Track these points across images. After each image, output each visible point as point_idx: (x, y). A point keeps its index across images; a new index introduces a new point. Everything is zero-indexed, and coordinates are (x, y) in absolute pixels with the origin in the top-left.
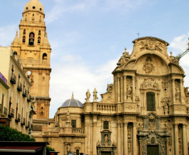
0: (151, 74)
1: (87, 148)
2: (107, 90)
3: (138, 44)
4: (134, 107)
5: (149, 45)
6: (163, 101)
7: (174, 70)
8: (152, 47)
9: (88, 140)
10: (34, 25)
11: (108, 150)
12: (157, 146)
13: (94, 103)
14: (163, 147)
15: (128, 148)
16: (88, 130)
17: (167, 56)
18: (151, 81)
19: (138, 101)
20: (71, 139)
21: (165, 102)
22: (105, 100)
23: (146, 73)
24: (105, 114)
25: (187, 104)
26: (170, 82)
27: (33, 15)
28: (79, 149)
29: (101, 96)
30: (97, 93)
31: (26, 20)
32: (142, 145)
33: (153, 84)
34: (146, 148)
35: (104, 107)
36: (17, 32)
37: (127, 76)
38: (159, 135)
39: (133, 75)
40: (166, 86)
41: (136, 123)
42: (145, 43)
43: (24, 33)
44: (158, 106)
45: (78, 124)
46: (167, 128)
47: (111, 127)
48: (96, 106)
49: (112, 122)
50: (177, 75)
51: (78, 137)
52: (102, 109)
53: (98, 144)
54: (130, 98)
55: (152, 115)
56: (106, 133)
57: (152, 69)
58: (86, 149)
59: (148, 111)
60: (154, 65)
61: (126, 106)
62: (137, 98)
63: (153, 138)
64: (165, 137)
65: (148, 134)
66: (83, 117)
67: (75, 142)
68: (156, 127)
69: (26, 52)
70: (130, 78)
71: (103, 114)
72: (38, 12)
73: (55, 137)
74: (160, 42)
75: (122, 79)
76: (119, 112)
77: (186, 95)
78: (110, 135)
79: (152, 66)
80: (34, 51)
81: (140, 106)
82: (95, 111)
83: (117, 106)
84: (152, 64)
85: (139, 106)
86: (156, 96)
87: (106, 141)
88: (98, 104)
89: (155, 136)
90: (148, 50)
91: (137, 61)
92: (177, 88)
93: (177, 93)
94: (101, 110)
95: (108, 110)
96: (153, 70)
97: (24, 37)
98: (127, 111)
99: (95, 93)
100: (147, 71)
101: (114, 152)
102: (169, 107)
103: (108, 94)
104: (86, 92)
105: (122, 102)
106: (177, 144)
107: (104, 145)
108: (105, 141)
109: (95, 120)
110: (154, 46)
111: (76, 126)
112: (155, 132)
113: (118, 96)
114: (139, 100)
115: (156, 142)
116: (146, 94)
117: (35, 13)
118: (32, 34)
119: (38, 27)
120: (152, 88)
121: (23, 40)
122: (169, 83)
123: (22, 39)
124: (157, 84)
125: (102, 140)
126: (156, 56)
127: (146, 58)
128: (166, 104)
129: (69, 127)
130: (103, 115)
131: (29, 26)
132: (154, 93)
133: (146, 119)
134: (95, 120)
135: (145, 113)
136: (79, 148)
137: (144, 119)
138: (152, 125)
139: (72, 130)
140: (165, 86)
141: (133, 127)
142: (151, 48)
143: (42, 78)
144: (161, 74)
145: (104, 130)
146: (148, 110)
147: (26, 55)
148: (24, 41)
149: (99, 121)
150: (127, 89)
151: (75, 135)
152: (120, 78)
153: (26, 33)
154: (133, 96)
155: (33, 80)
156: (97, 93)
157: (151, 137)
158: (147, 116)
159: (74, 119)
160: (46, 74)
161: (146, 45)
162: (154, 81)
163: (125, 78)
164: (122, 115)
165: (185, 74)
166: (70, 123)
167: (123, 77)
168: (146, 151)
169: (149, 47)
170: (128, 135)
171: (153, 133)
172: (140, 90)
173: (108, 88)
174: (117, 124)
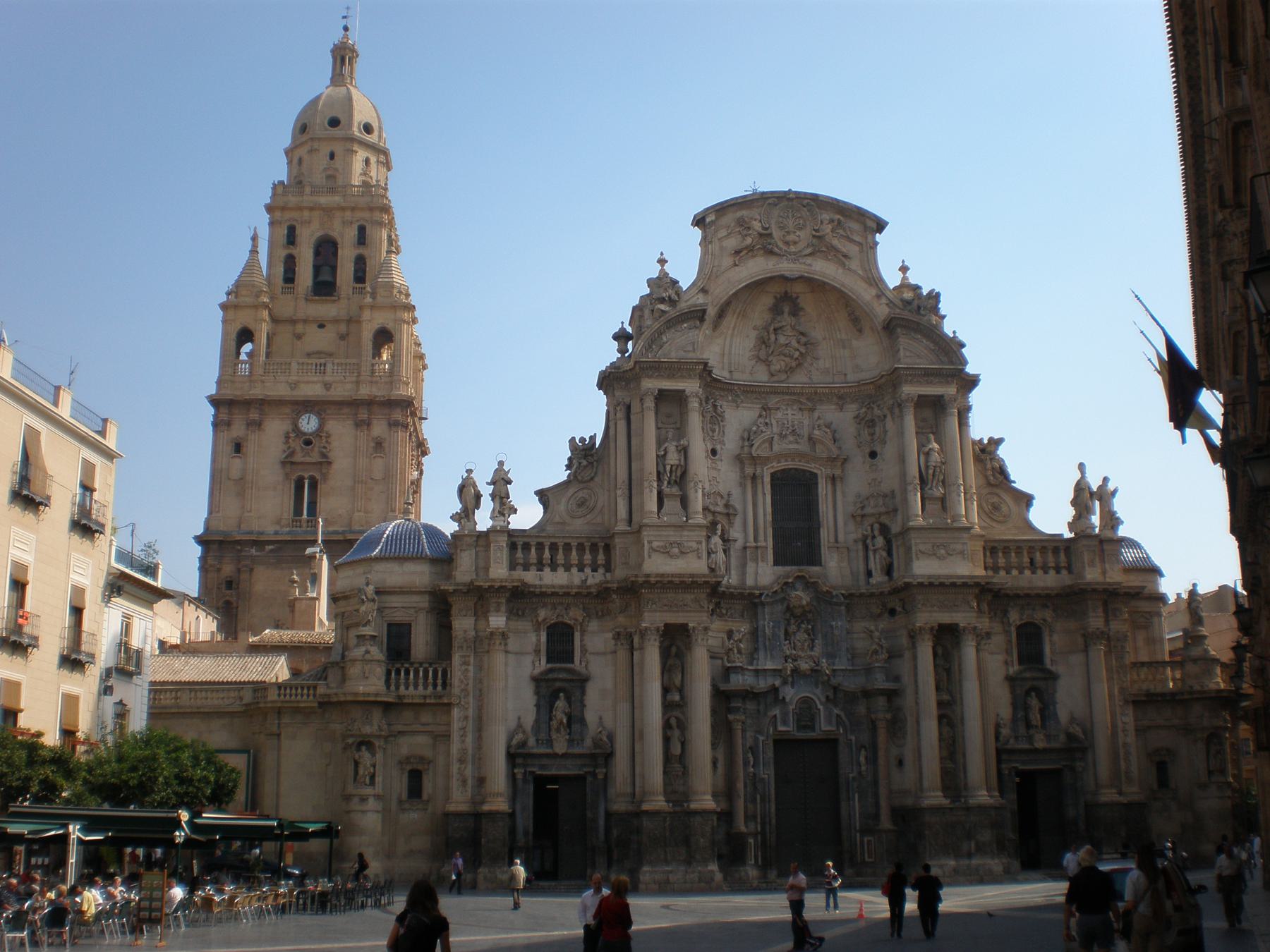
0: (799, 379)
1: (462, 761)
2: (568, 467)
3: (723, 233)
4: (694, 545)
5: (777, 234)
6: (859, 512)
7: (912, 353)
8: (795, 243)
9: (466, 718)
10: (337, 199)
11: (570, 769)
12: (830, 743)
13: (492, 537)
14: (864, 747)
15: (667, 758)
16: (460, 667)
17: (875, 280)
18: (799, 416)
19: (728, 515)
20: (377, 715)
21: (873, 515)
22: (557, 519)
23: (772, 375)
24: (553, 586)
25: (994, 524)
26: (892, 413)
27: (332, 156)
28: (420, 767)
29: (540, 500)
30: (510, 482)
31: (300, 182)
32: (744, 738)
33: (805, 432)
34: (770, 754)
35: (547, 554)
36: (254, 239)
37: (660, 391)
38: (835, 689)
39: (691, 386)
40: (876, 437)
41: (706, 629)
42: (757, 226)
43: (291, 238)
44: (836, 541)
45: (421, 642)
46: (876, 652)
47: (584, 651)
48: (500, 548)
49: (593, 625)
50: (928, 375)
51: (418, 707)
52: (540, 566)
53: (519, 737)
54: (679, 504)
55: (798, 585)
56: (558, 684)
57: (801, 354)
58: (455, 768)
59: (780, 567)
60: (817, 333)
61: (650, 542)
62: (721, 503)
63: (806, 703)
64: (867, 694)
65: (777, 683)
66: (441, 605)
67: (401, 733)
69: (300, 328)
70: (679, 398)
71: (541, 587)
72: (352, 140)
73: (297, 710)
74: (838, 217)
75: (635, 408)
76: (620, 573)
77: (986, 477)
78: (583, 693)
79: (803, 340)
80: (336, 321)
81: (739, 544)
82: (499, 571)
83: (614, 547)
84: (802, 329)
86: (823, 489)
87: (561, 723)
88: (520, 542)
89: (818, 691)
91: (721, 315)
92: (929, 442)
93: (927, 467)
94: (534, 568)
95: (567, 568)
96: (809, 359)
97: (290, 263)
98: (656, 565)
99: (497, 483)
100: (778, 367)
101: (600, 777)
102: (889, 542)
103: (571, 491)
104: (460, 482)
105: (635, 526)
106: (930, 728)
107: (550, 742)
108: (554, 723)
109: (497, 621)
110: (804, 235)
111: (409, 650)
112: (816, 671)
113: (619, 492)
114: (731, 511)
115: (824, 726)
116: (767, 479)
117: (338, 149)
118: (326, 249)
119: (353, 209)
120: (804, 447)
121: (286, 272)
122: (889, 417)
123: (280, 270)
124: (828, 426)
125: (537, 721)
126: (817, 286)
127: (767, 301)
128: (876, 526)
129: (368, 657)
130: (543, 594)
131: (311, 209)
132: (811, 473)
134: (497, 621)
135: (764, 573)
136: (422, 759)
137: (760, 610)
138: (801, 636)
139: (388, 673)
140: (872, 434)
141: (689, 647)
142: (793, 249)
143: (373, 444)
144: (851, 377)
145: (549, 666)
146: (776, 563)
147: (299, 343)
148: (290, 277)
149: (524, 625)
150: (661, 459)
151: (399, 697)
152: (628, 408)
153: (298, 240)
154: (691, 494)
155: (329, 455)
156: (510, 482)
157: (790, 694)
158: (775, 592)
159: (399, 617)
160: (390, 425)
161: (765, 235)
162: (816, 414)
163: (650, 403)
164: (634, 591)
165: (970, 369)
166: (373, 637)
167: (641, 400)
168: (771, 772)
169: (781, 244)
170: (666, 690)
172: (739, 459)
173: (570, 459)
174: (617, 636)
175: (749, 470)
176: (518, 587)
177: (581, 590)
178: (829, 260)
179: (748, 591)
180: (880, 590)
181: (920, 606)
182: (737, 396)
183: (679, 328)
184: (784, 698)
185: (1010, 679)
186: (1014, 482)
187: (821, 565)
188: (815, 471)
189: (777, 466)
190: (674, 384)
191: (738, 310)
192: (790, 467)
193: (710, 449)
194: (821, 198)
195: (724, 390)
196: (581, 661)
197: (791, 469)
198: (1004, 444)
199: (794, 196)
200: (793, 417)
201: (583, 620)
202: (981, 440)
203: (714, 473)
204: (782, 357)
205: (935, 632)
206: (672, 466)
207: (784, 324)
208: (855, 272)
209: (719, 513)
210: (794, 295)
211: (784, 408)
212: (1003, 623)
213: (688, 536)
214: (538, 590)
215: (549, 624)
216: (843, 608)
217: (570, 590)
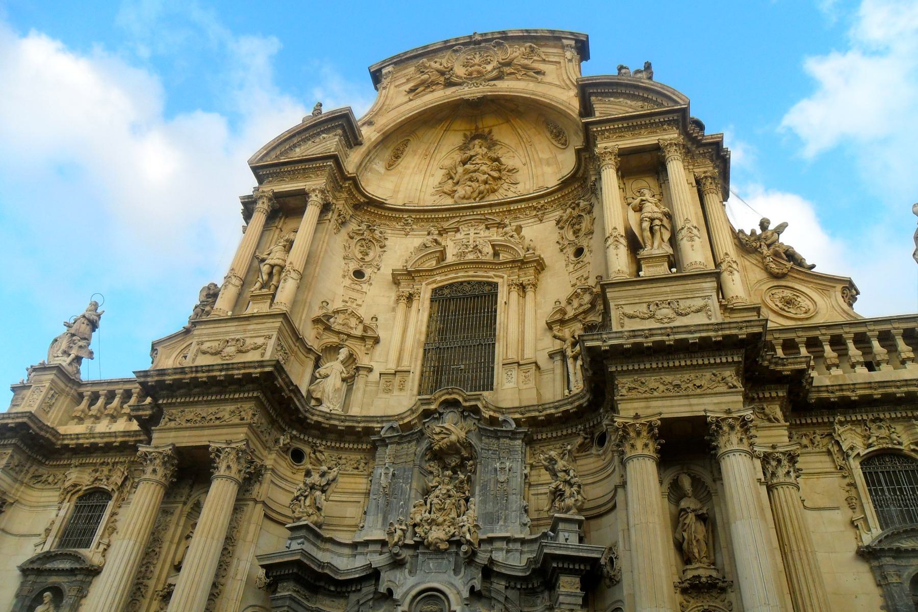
5: (460, 71)
50: (631, 124)
56: (53, 579)
65: (378, 560)
68: (484, 502)
85: (370, 370)
90: (453, 89)
114: (370, 333)
132: (489, 284)
133: (390, 449)
158: (408, 426)
171: (438, 552)
175: (406, 289)
176: (24, 424)
177: (127, 439)
178: (519, 80)
179: (362, 425)
180: (577, 404)
181: (624, 392)
182: (407, 224)
183: (317, 140)
184: (390, 592)
185: (866, 554)
186: (813, 266)
187: (492, 389)
188: (495, 280)
189: (441, 279)
190: (296, 185)
191: (420, 151)
192: (460, 280)
193: (353, 266)
194: (510, 35)
195: (390, 218)
196: (99, 543)
197: (462, 283)
198: (786, 229)
199: (480, 38)
200: (476, 235)
201: (123, 483)
202: (753, 233)
203: (355, 295)
204: (469, 183)
205: (656, 431)
206: (272, 266)
207: (472, 153)
208: (550, 84)
209: (349, 336)
210: (487, 130)
211: (466, 229)
212: (829, 453)
213: (254, 330)
214: (74, 442)
215: (81, 493)
216: (519, 442)
217: (113, 439)
